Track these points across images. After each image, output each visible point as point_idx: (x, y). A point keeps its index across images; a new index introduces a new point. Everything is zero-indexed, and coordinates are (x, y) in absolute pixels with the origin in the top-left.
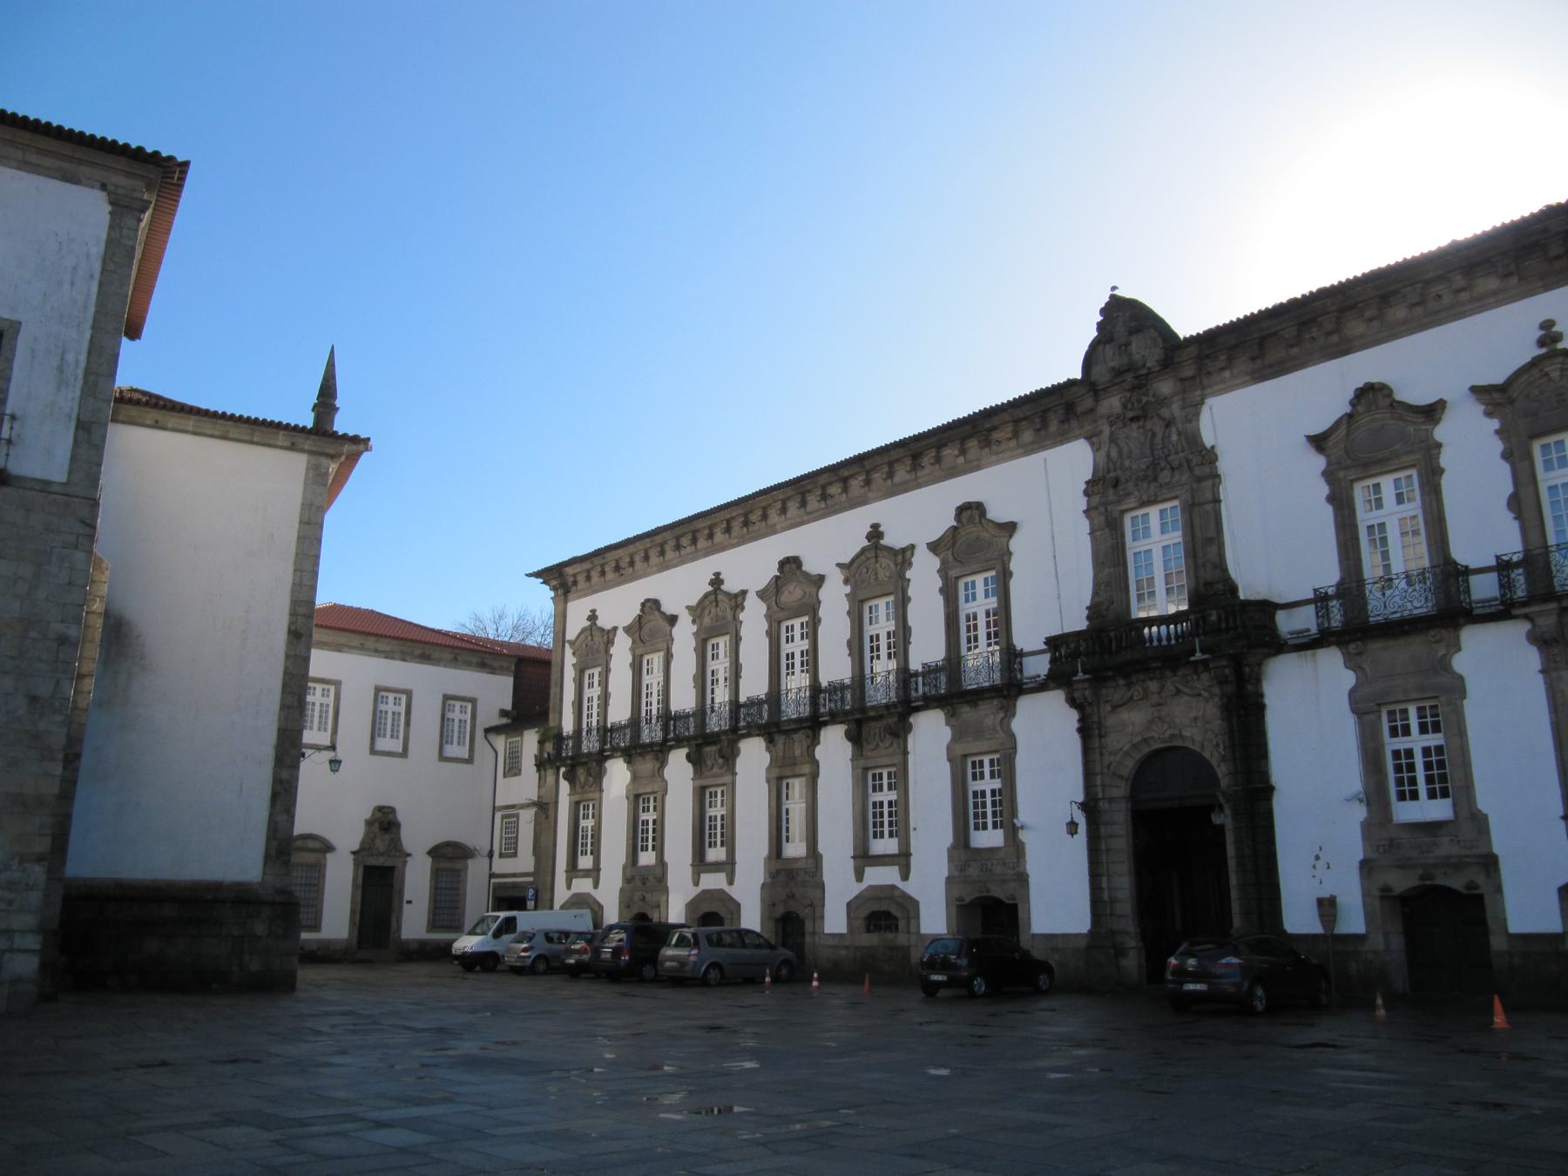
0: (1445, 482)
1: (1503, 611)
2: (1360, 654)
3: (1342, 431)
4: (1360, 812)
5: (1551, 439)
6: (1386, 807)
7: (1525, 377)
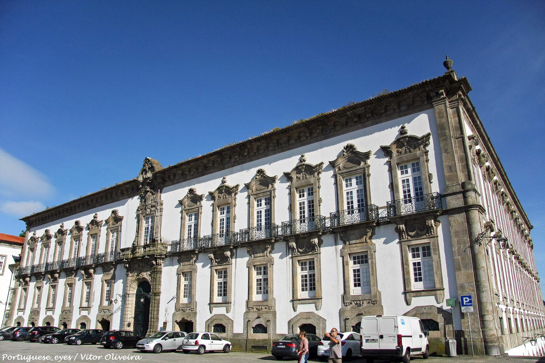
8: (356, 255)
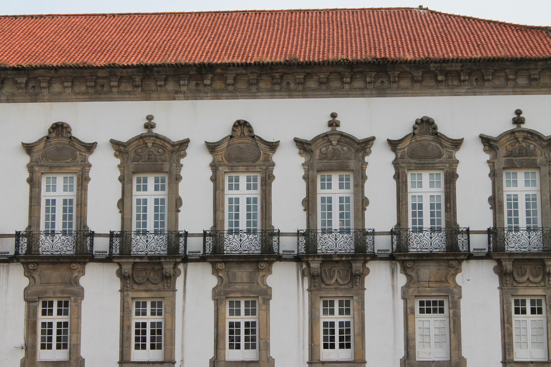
0: (91, 186)
1: (108, 259)
2: (34, 270)
3: (42, 145)
4: (22, 354)
5: (142, 176)
6: (34, 354)
7: (137, 142)
8: (425, 300)
